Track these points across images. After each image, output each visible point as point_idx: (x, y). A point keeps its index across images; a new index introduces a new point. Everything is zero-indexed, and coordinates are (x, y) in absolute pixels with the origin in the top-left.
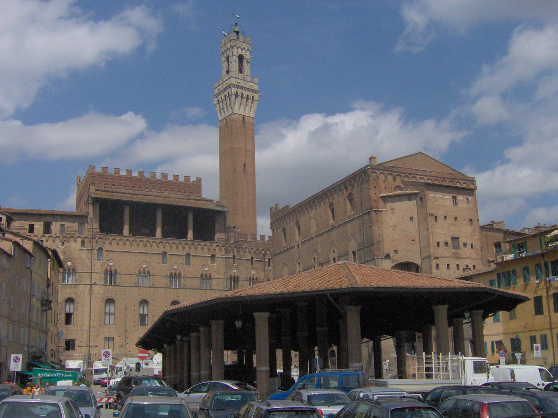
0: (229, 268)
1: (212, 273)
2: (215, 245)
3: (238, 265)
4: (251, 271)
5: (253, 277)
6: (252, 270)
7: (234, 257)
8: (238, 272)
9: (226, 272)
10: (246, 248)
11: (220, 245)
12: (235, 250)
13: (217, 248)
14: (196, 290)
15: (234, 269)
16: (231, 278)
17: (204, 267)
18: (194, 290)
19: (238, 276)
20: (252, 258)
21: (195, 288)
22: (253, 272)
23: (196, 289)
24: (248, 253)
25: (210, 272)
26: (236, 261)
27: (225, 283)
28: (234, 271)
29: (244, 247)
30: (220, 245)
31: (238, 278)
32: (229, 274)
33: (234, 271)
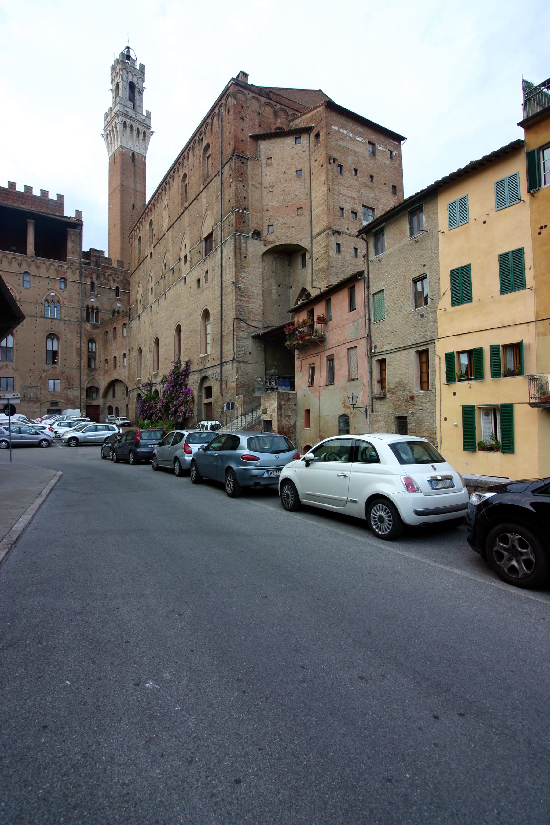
0: (86, 296)
1: (61, 300)
2: (66, 267)
3: (97, 294)
4: (115, 304)
5: (119, 310)
6: (117, 302)
7: (93, 284)
8: (98, 302)
9: (81, 301)
10: (110, 275)
11: (74, 268)
12: (94, 277)
13: (69, 271)
14: (38, 319)
15: (93, 298)
16: (88, 308)
17: (49, 292)
18: (34, 319)
19: (97, 307)
20: (117, 288)
21: (36, 315)
22: (118, 305)
23: (37, 317)
24: (112, 282)
25: (58, 299)
26: (96, 289)
27: (79, 313)
28: (92, 300)
29: (106, 274)
30: (74, 268)
31: (97, 309)
32: (85, 303)
33: (92, 300)
